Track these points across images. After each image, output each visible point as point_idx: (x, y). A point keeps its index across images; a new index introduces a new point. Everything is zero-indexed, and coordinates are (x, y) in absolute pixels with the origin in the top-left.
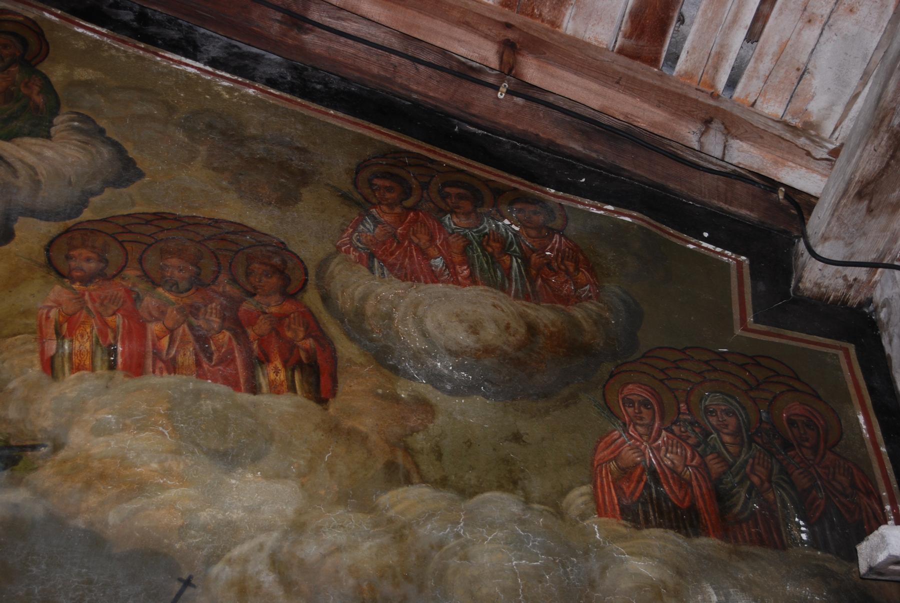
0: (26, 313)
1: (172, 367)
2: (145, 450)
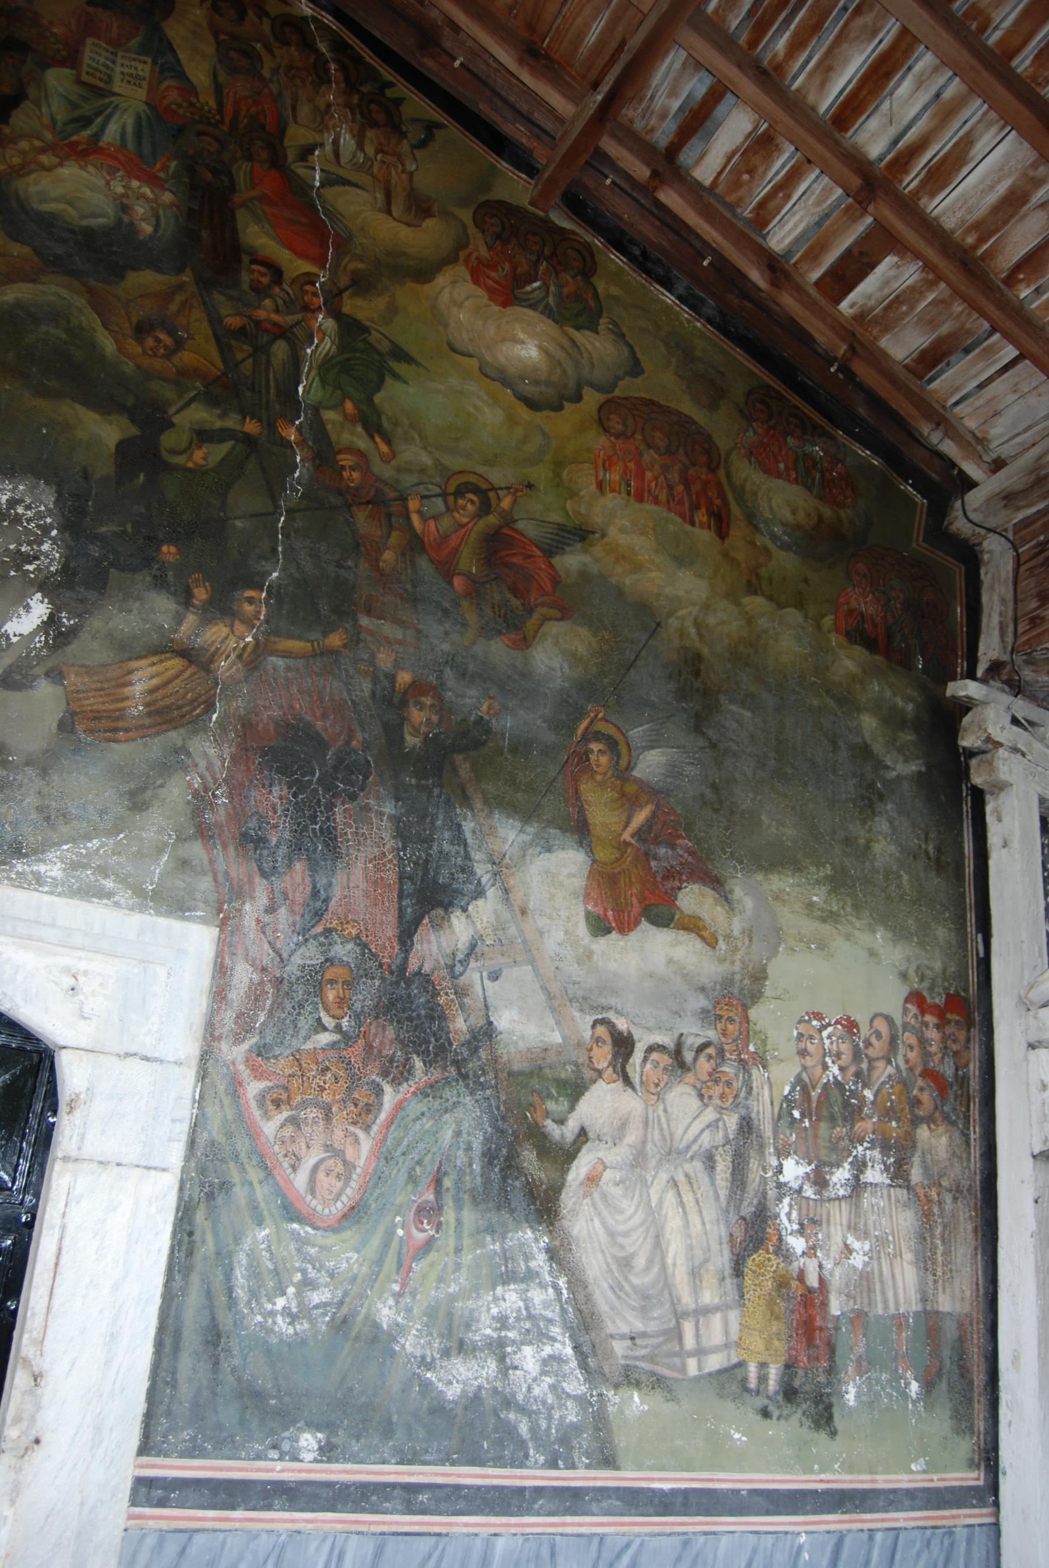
0: (589, 450)
1: (656, 501)
2: (642, 545)
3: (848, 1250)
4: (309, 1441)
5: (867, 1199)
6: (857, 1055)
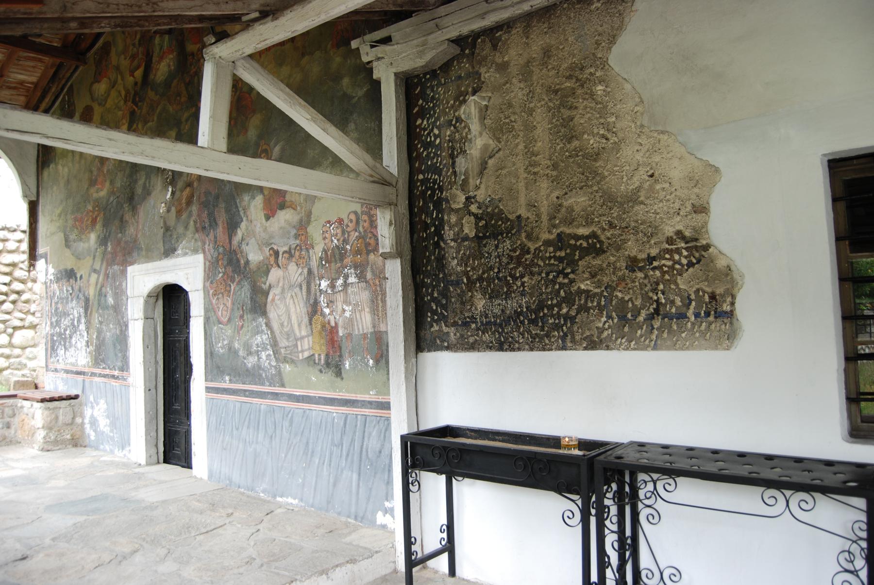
3: (344, 311)
4: (227, 378)
5: (350, 290)
6: (343, 232)
